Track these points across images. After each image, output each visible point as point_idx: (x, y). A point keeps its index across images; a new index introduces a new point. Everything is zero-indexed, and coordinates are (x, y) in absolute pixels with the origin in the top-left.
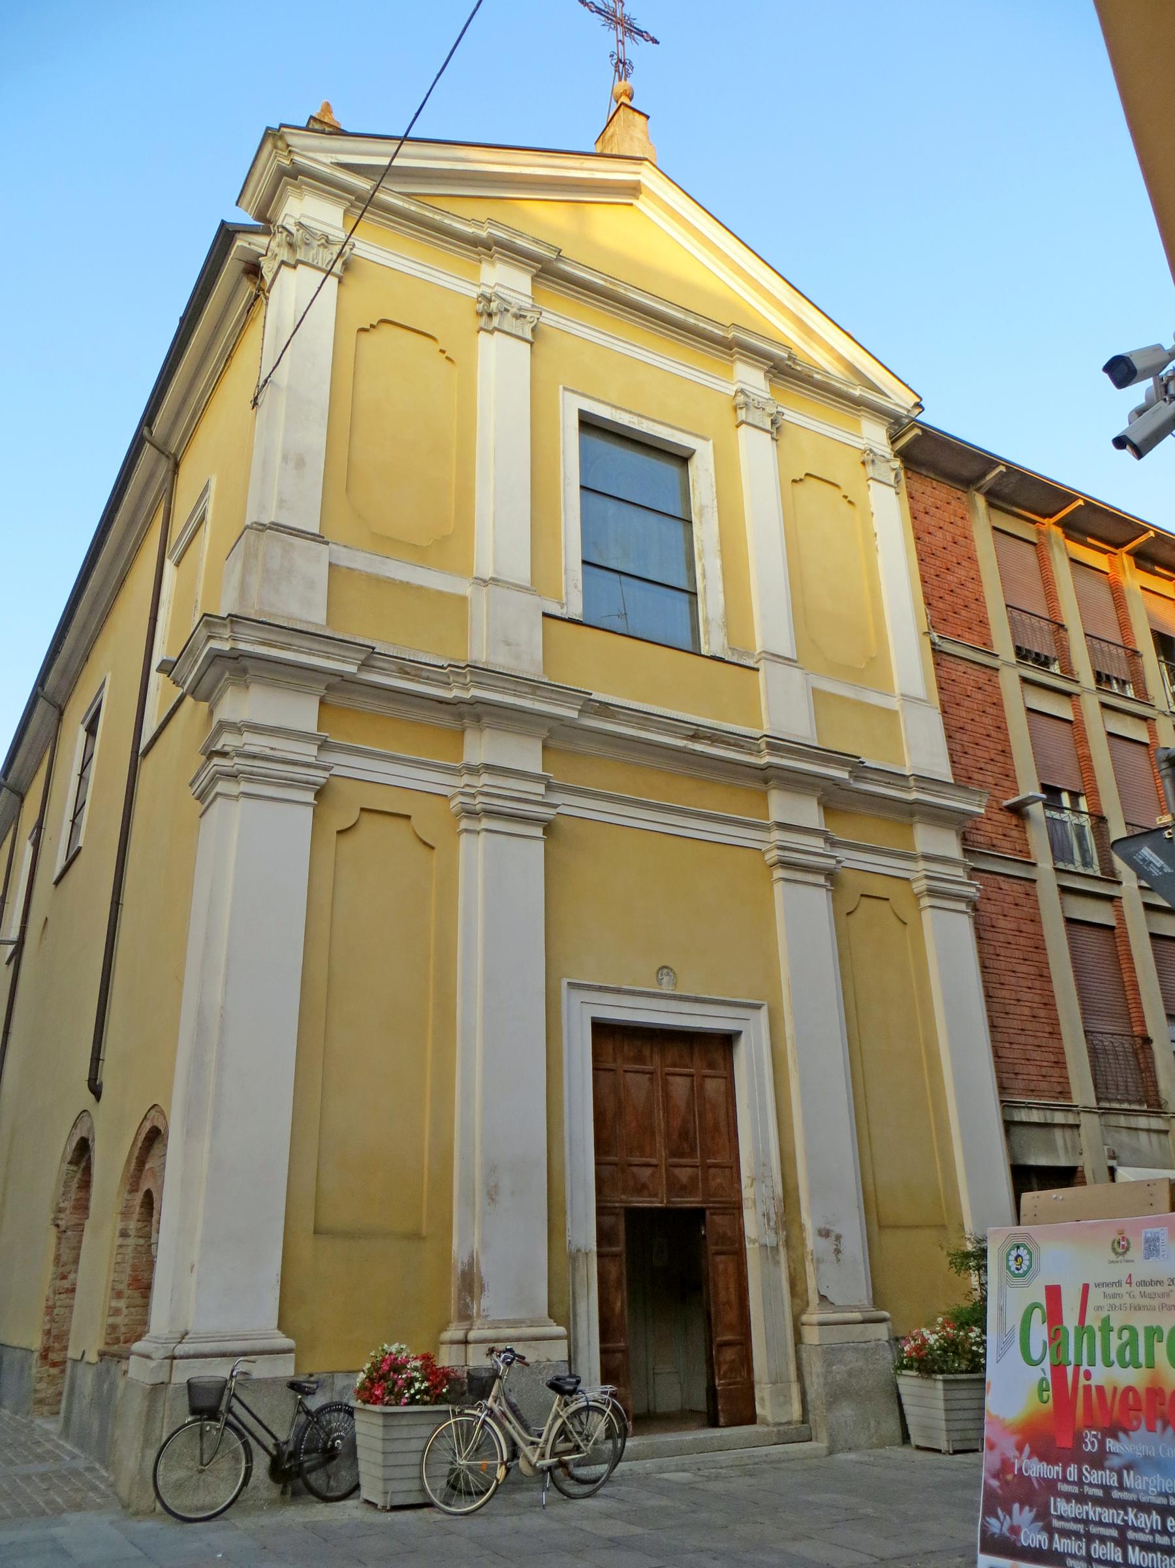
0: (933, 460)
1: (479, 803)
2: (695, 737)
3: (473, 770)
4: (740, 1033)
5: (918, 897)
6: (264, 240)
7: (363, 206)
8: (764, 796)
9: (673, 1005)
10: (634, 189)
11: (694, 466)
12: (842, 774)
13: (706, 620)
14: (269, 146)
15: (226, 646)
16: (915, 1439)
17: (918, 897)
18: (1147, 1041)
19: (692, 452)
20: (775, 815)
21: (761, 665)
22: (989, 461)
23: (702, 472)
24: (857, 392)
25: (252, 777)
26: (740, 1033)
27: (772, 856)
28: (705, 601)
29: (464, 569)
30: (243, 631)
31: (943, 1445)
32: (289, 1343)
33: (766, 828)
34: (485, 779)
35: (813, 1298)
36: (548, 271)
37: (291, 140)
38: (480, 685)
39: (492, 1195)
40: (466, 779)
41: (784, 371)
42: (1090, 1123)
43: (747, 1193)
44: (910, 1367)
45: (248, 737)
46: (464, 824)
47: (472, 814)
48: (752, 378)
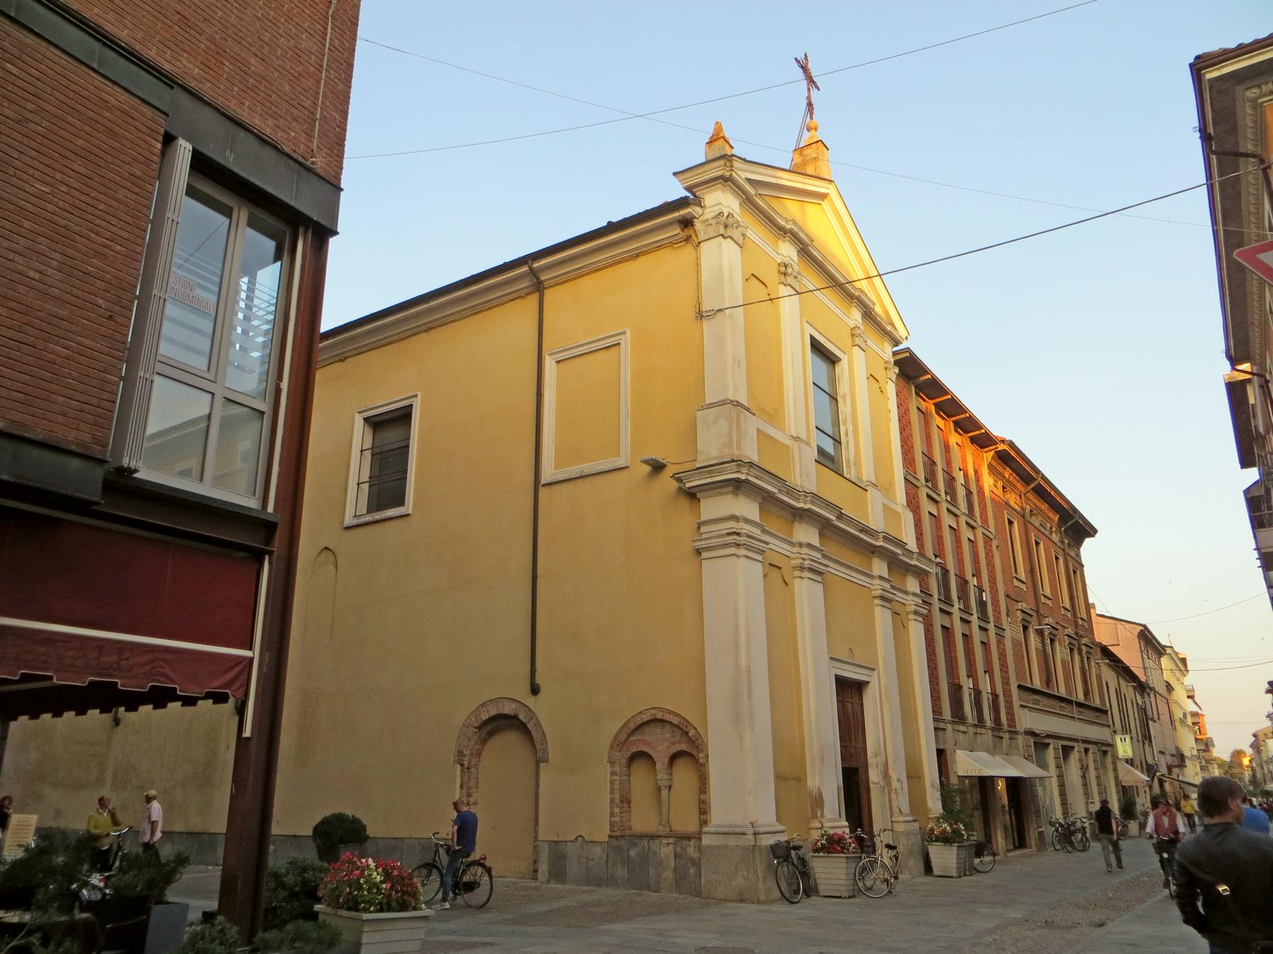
0: (910, 370)
1: (807, 563)
2: (861, 531)
3: (801, 545)
4: (867, 683)
5: (908, 613)
6: (698, 209)
7: (748, 201)
8: (870, 559)
9: (858, 670)
10: (823, 196)
11: (838, 367)
12: (899, 552)
13: (848, 460)
14: (721, 162)
15: (743, 477)
16: (936, 872)
17: (908, 613)
18: (961, 687)
19: (839, 360)
20: (876, 572)
21: (869, 489)
22: (925, 370)
23: (842, 368)
24: (889, 328)
25: (747, 547)
26: (867, 683)
27: (879, 592)
28: (847, 449)
29: (782, 430)
30: (753, 471)
31: (954, 874)
32: (783, 828)
33: (872, 577)
34: (805, 550)
35: (896, 810)
36: (805, 250)
37: (735, 164)
38: (812, 502)
39: (823, 760)
40: (796, 549)
41: (868, 314)
42: (949, 727)
43: (871, 760)
44: (937, 840)
45: (742, 525)
46: (797, 573)
47: (802, 568)
48: (856, 316)
